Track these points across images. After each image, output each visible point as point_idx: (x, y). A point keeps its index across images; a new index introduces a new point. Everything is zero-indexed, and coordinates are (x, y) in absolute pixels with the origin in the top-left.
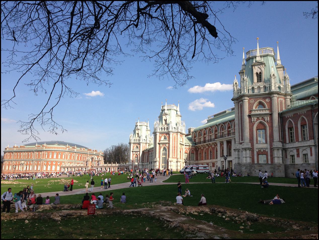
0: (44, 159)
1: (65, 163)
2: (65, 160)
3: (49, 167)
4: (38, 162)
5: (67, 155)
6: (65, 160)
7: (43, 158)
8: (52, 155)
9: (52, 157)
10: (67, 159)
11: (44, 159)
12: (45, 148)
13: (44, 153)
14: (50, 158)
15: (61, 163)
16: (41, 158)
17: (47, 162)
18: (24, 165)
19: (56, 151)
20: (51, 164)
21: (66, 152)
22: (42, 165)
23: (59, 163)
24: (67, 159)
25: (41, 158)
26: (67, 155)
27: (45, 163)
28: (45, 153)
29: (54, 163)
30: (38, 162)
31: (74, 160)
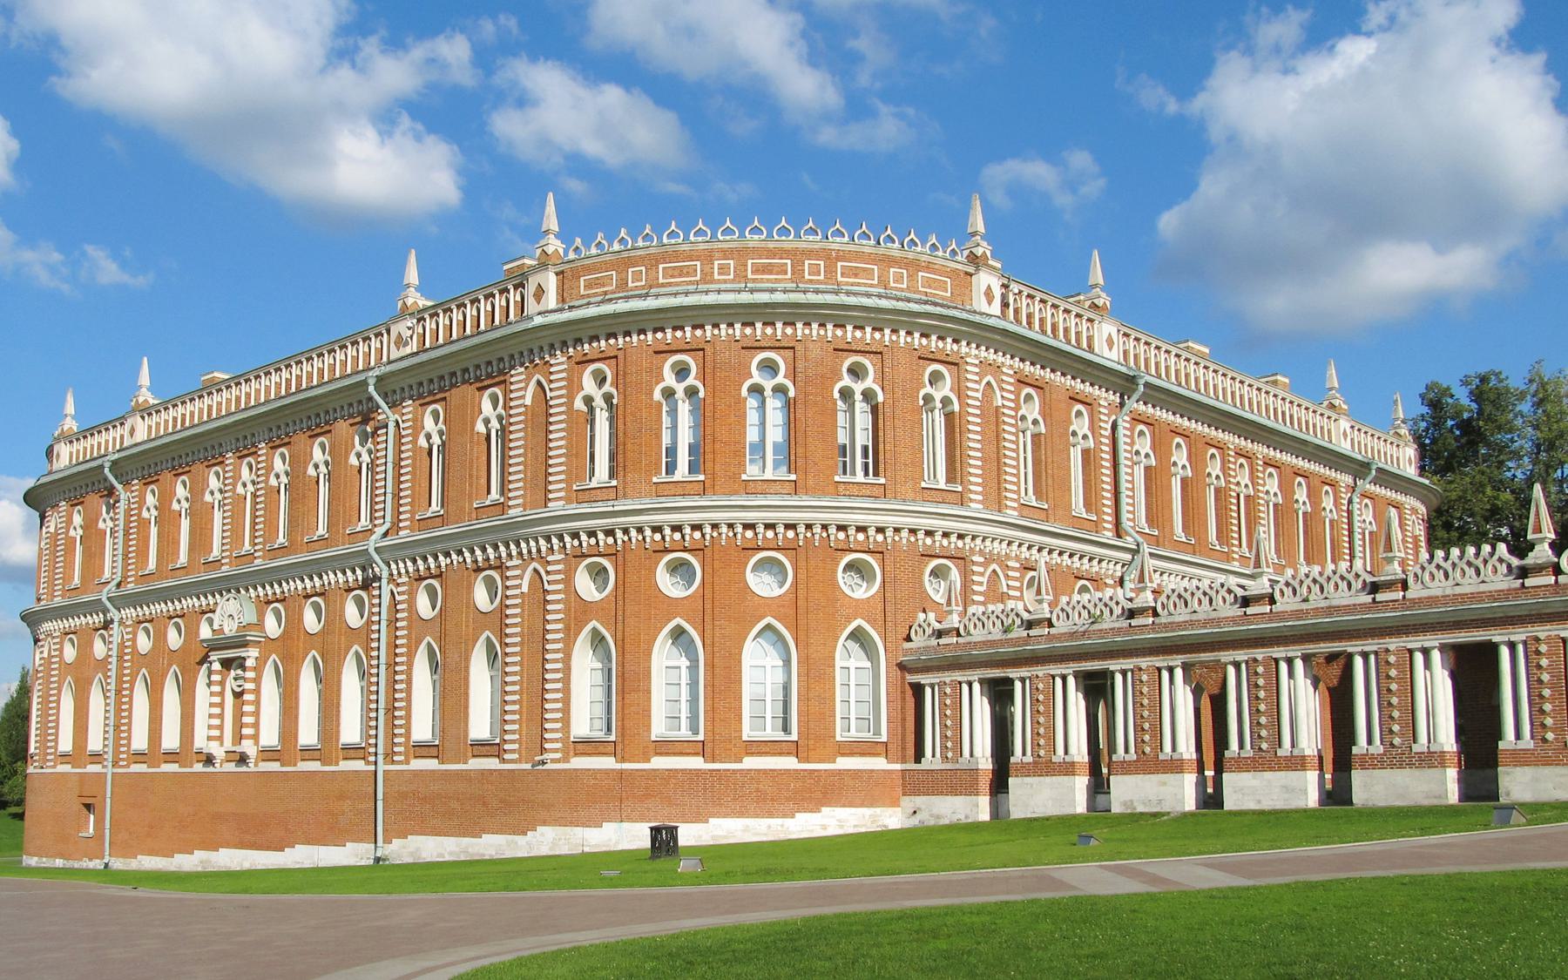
0: (557, 507)
1: (981, 583)
2: (976, 508)
3: (669, 672)
4: (450, 586)
5: (993, 417)
6: (976, 508)
7: (541, 490)
8: (702, 414)
9: (716, 454)
10: (995, 497)
11: (557, 507)
12: (551, 301)
13: (556, 393)
14: (682, 489)
15: (901, 563)
16: (502, 507)
17: (627, 562)
18: (252, 654)
19: (766, 313)
20: (705, 609)
21: (972, 353)
22: (537, 641)
23: (860, 591)
24: (995, 497)
25: (502, 507)
26: (993, 417)
27: (586, 586)
28: (573, 386)
29: (763, 585)
30: (450, 586)
31: (1108, 536)
